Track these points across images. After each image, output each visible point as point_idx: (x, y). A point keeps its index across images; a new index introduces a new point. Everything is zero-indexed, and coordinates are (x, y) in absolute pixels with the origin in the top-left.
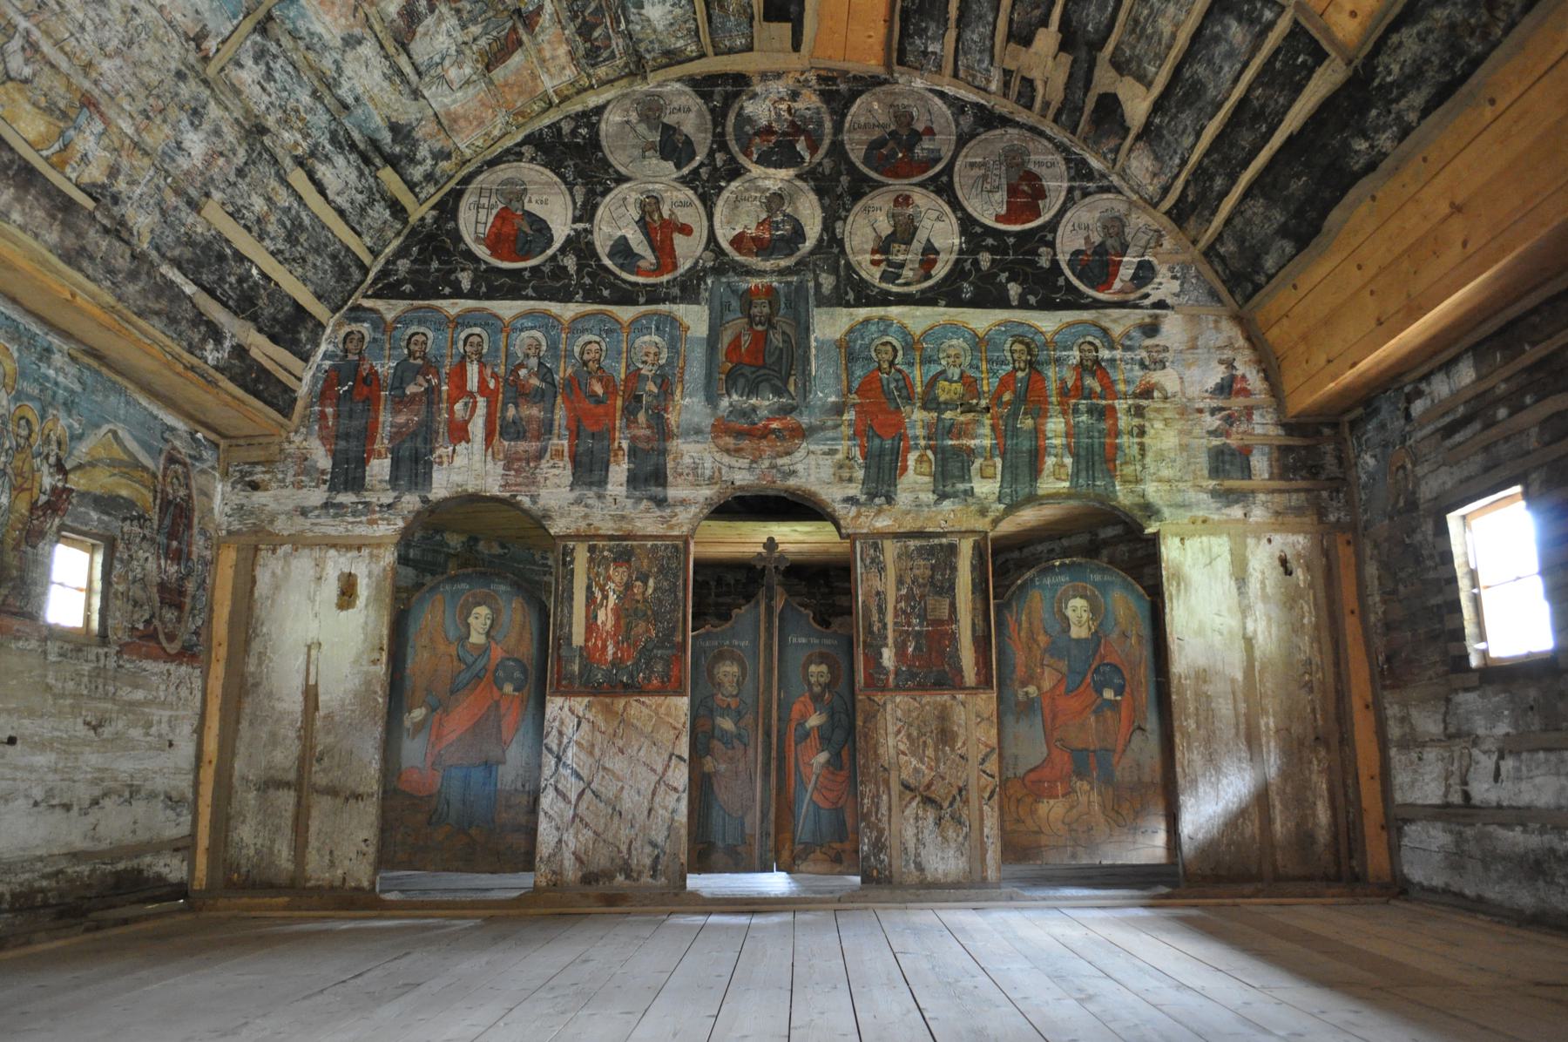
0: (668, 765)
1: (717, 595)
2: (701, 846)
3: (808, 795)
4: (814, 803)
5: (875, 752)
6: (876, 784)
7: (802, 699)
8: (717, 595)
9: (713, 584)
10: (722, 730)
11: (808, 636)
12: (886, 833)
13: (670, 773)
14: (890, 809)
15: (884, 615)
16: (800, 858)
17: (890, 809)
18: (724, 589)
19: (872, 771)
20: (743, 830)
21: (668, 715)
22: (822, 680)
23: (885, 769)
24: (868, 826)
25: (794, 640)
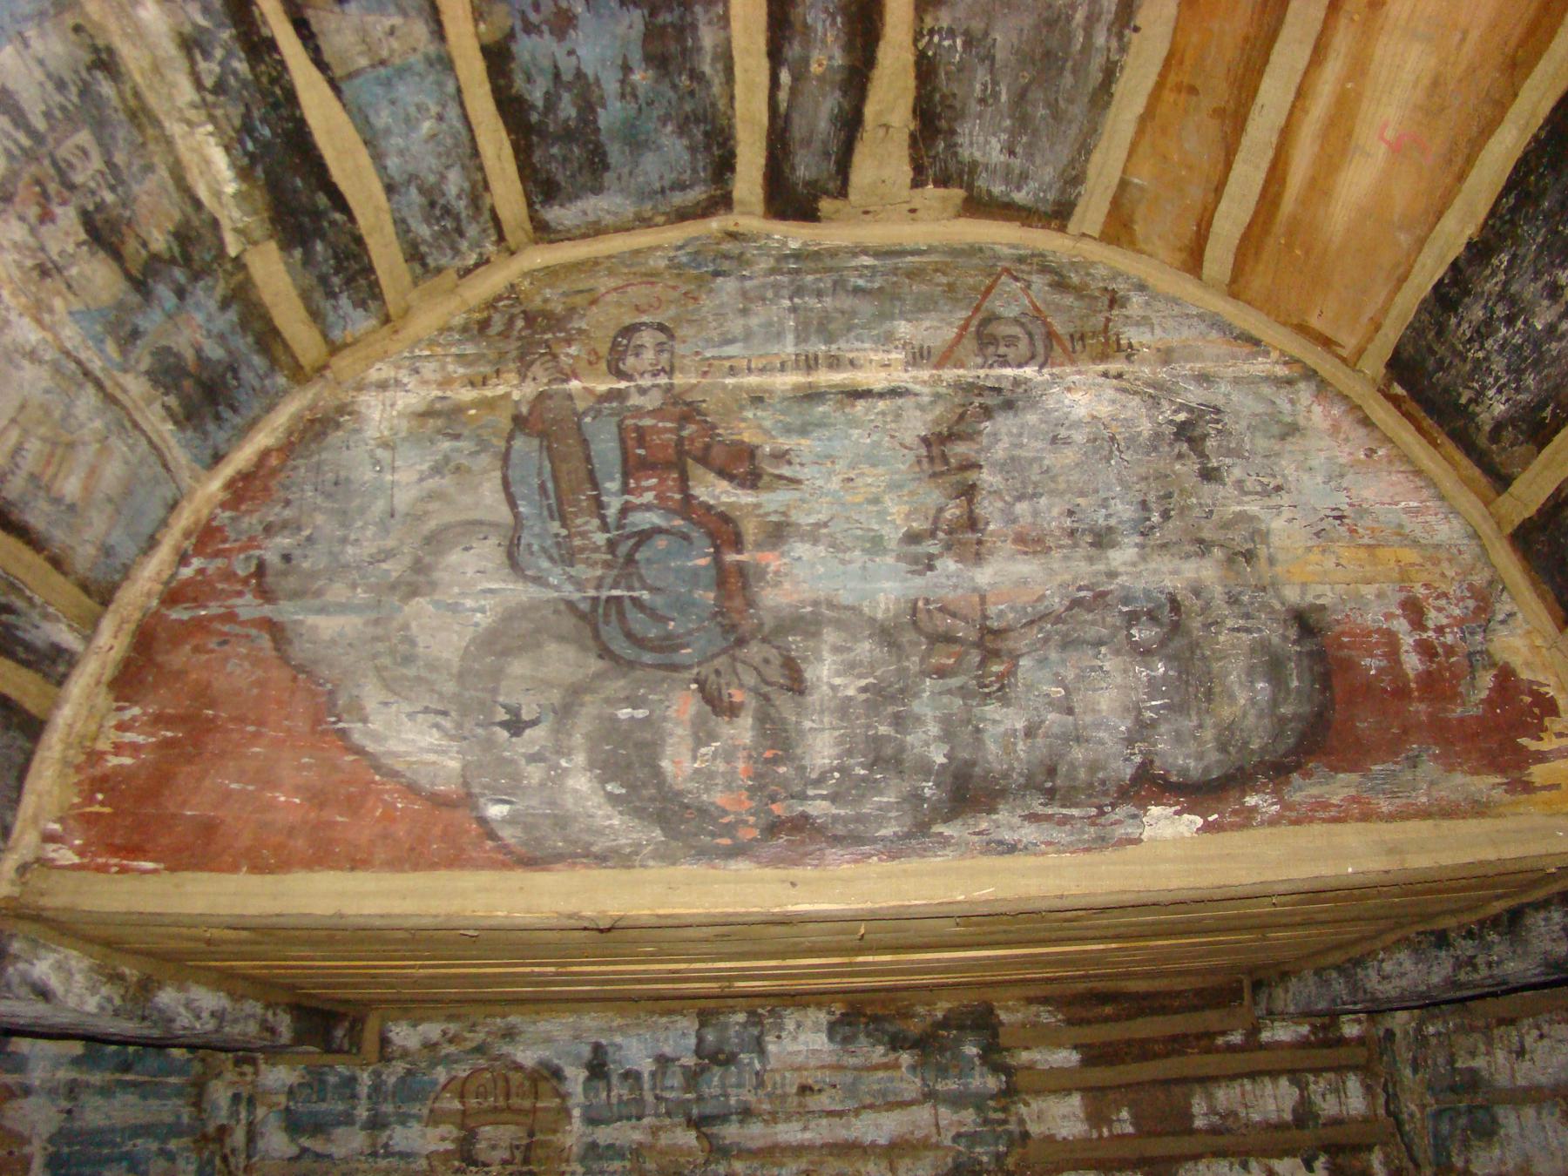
1: (592, 1120)
8: (592, 1120)
9: (576, 1077)
18: (620, 1091)
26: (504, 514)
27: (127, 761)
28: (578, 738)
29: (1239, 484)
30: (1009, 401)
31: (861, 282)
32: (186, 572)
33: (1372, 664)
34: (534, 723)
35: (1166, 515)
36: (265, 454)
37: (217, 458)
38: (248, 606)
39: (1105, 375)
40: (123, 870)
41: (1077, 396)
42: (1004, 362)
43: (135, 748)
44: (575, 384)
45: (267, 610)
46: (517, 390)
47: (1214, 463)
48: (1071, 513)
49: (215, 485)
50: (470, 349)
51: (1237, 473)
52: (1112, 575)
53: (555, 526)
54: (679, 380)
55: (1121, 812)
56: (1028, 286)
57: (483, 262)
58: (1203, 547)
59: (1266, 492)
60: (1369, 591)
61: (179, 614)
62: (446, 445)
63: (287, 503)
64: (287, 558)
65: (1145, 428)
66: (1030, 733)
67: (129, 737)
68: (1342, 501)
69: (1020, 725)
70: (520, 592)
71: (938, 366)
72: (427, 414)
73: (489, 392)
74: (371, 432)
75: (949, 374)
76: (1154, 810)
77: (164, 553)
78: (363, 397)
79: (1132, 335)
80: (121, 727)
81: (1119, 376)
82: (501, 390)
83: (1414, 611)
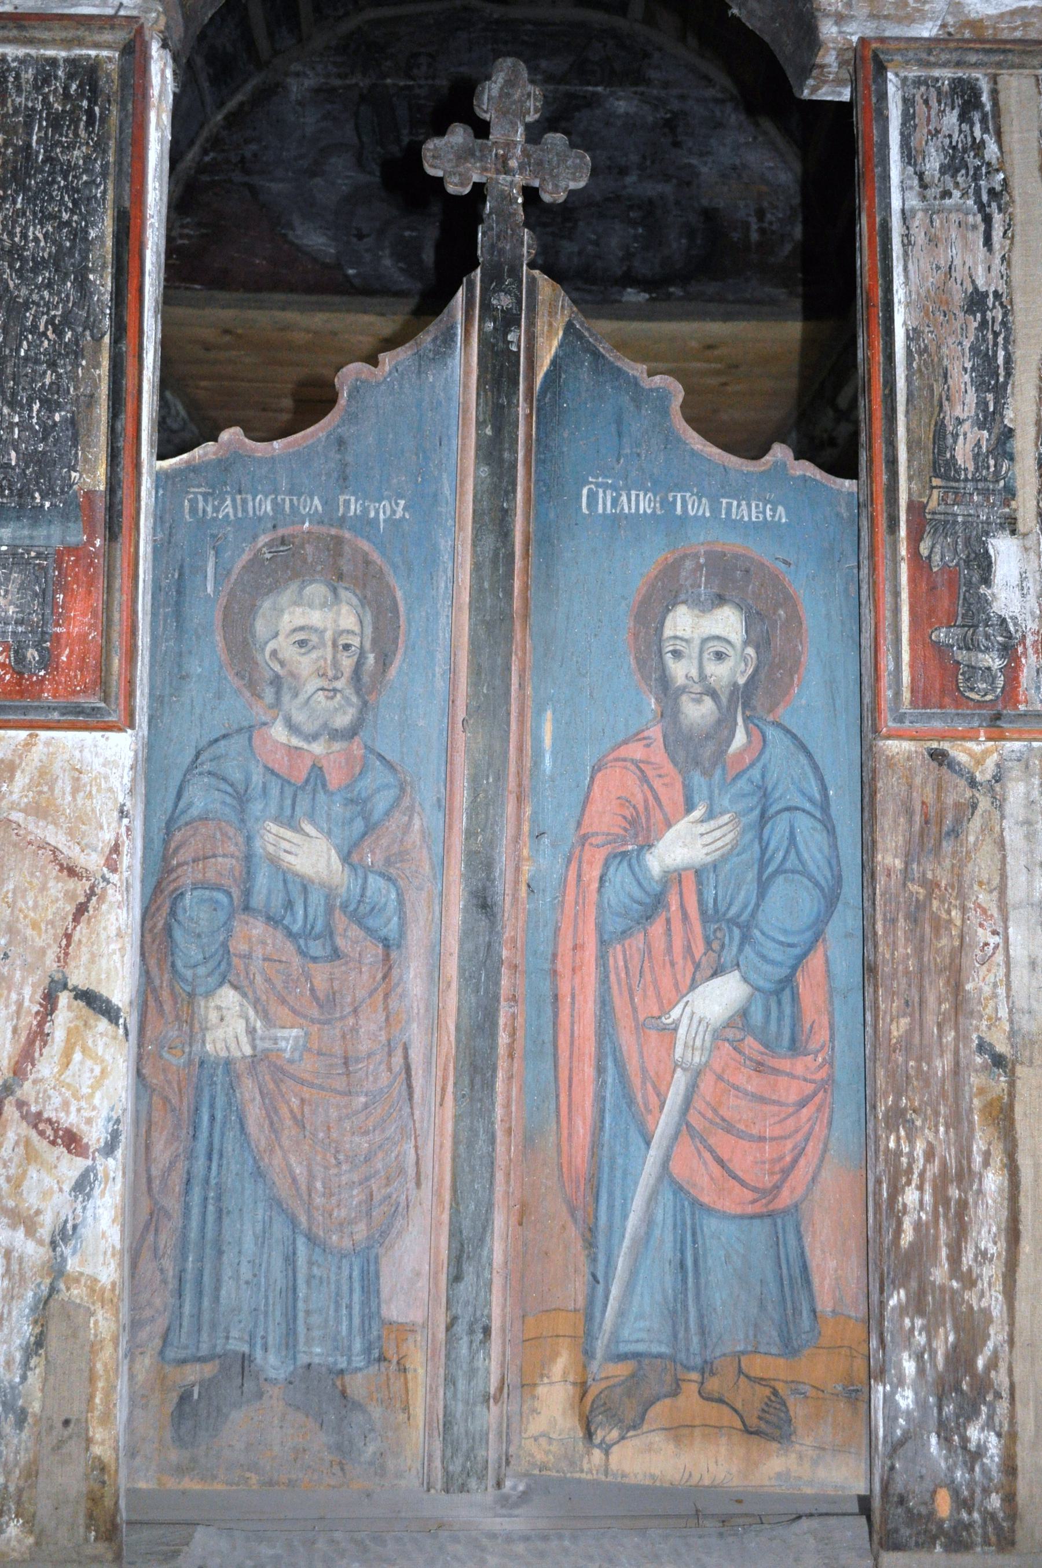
0: (39, 1036)
2: (192, 1374)
3: (654, 1154)
4: (679, 1189)
5: (957, 988)
6: (957, 1120)
7: (634, 749)
10: (284, 875)
11: (659, 486)
12: (996, 1336)
13: (46, 1067)
14: (1013, 1234)
15: (1000, 391)
16: (613, 1417)
17: (1013, 1234)
19: (942, 1065)
20: (371, 1314)
21: (41, 810)
22: (720, 673)
23: (998, 1061)
24: (917, 1305)
25: (604, 504)
26: (356, 140)
27: (186, 242)
28: (387, 244)
29: (690, 150)
30: (591, 102)
31: (526, 38)
32: (207, 159)
33: (735, 236)
34: (368, 235)
35: (653, 162)
36: (242, 104)
37: (222, 104)
38: (238, 177)
39: (636, 93)
40: (186, 288)
41: (621, 103)
42: (589, 84)
43: (188, 236)
44: (389, 81)
45: (246, 179)
46: (361, 81)
47: (679, 139)
48: (610, 158)
49: (219, 117)
50: (339, 59)
51: (690, 144)
52: (625, 187)
53: (379, 149)
54: (438, 82)
55: (615, 289)
56: (605, 45)
57: (347, 14)
58: (667, 178)
59: (701, 155)
60: (741, 204)
61: (205, 178)
62: (329, 107)
63: (255, 129)
64: (255, 155)
65: (650, 119)
66: (580, 253)
67: (186, 231)
68: (738, 162)
69: (576, 249)
70: (363, 178)
71: (559, 83)
72: (317, 91)
73: (348, 82)
74: (293, 97)
75: (562, 88)
76: (629, 290)
77: (196, 149)
78: (289, 80)
79: (653, 74)
80: (182, 226)
81: (642, 94)
82: (354, 81)
83: (760, 214)
